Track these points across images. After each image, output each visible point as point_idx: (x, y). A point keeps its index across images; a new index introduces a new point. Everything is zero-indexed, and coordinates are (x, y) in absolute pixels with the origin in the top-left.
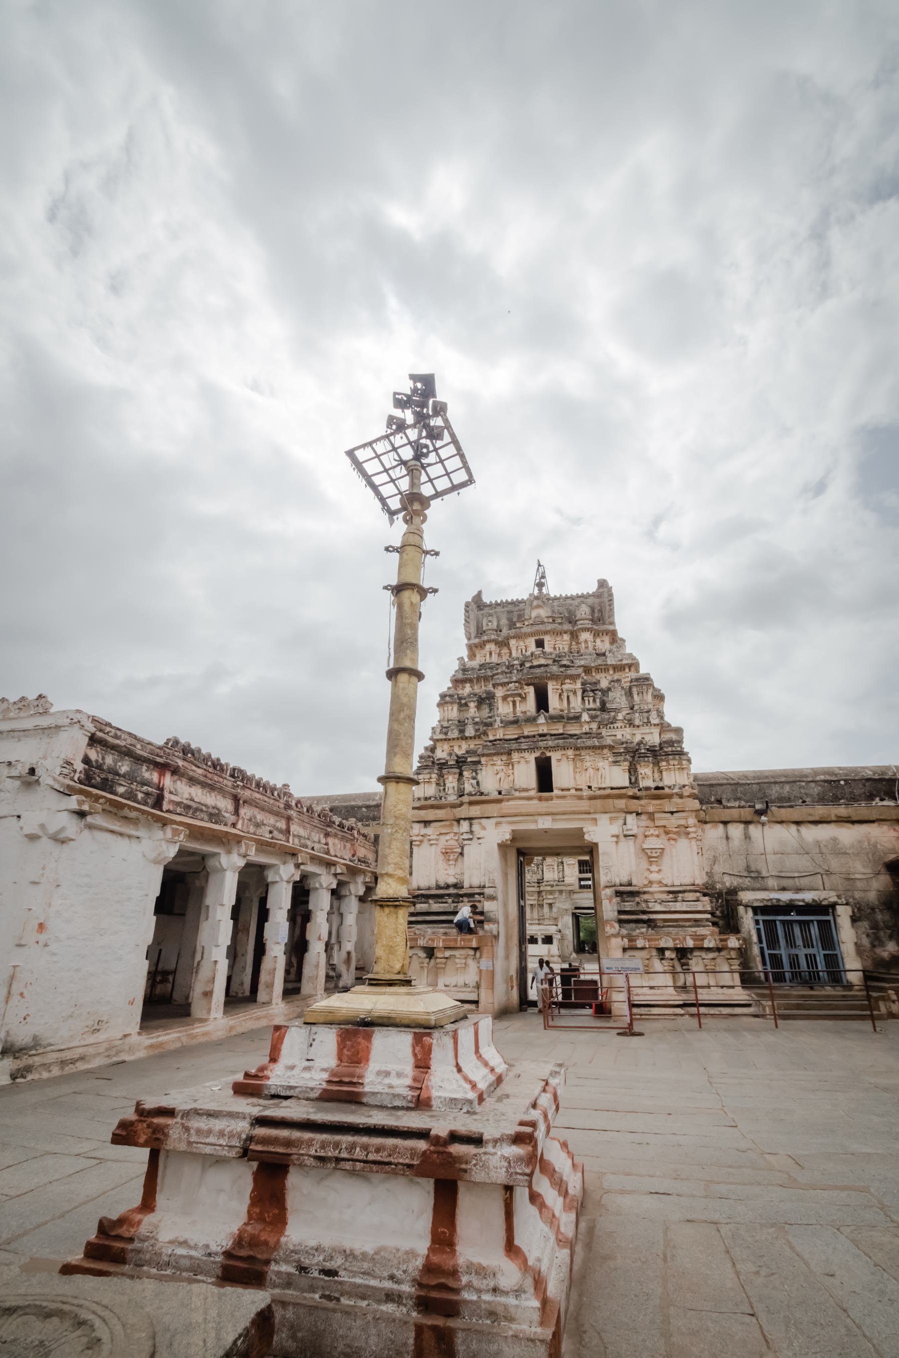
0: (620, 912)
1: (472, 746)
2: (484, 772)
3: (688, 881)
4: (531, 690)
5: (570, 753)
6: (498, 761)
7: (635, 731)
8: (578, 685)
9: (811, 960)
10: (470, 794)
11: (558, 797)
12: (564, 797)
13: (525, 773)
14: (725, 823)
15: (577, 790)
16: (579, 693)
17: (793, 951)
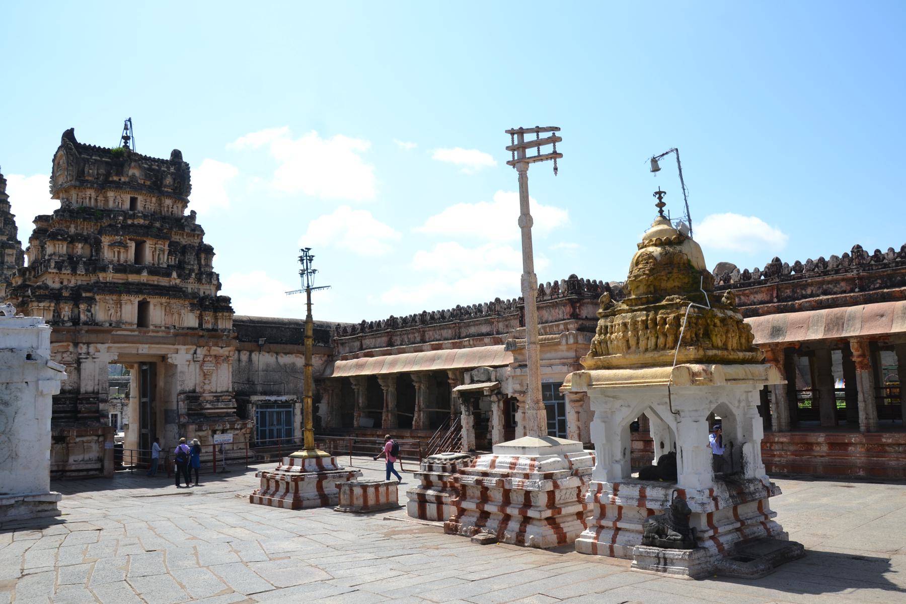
0: (189, 409)
1: (79, 283)
2: (97, 308)
3: (225, 389)
4: (132, 245)
5: (164, 300)
6: (111, 299)
7: (201, 287)
8: (166, 247)
9: (279, 431)
10: (85, 323)
11: (153, 331)
12: (158, 332)
13: (129, 310)
14: (239, 351)
15: (166, 328)
16: (166, 253)
17: (272, 428)
